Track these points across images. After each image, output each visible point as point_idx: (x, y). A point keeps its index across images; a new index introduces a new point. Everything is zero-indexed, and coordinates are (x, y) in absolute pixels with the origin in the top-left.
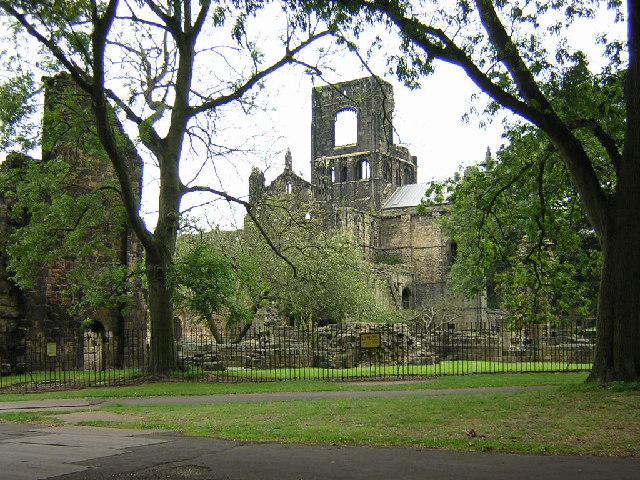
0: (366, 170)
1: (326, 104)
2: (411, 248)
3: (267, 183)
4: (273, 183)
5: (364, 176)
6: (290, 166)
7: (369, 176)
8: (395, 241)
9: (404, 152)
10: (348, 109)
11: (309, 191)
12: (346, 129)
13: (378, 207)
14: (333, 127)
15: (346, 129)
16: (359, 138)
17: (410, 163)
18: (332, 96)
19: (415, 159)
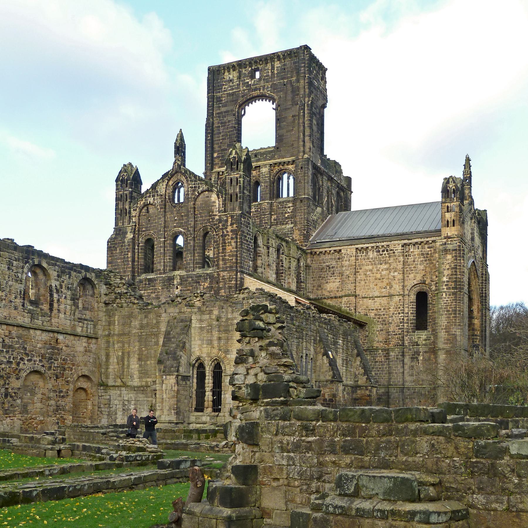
0: (288, 186)
3: (145, 187)
4: (154, 186)
5: (285, 195)
6: (183, 160)
7: (291, 194)
8: (332, 285)
9: (336, 166)
10: (262, 97)
11: (214, 197)
12: (259, 125)
13: (306, 237)
14: (239, 123)
15: (259, 125)
16: (279, 138)
17: (344, 184)
18: (239, 78)
19: (349, 180)
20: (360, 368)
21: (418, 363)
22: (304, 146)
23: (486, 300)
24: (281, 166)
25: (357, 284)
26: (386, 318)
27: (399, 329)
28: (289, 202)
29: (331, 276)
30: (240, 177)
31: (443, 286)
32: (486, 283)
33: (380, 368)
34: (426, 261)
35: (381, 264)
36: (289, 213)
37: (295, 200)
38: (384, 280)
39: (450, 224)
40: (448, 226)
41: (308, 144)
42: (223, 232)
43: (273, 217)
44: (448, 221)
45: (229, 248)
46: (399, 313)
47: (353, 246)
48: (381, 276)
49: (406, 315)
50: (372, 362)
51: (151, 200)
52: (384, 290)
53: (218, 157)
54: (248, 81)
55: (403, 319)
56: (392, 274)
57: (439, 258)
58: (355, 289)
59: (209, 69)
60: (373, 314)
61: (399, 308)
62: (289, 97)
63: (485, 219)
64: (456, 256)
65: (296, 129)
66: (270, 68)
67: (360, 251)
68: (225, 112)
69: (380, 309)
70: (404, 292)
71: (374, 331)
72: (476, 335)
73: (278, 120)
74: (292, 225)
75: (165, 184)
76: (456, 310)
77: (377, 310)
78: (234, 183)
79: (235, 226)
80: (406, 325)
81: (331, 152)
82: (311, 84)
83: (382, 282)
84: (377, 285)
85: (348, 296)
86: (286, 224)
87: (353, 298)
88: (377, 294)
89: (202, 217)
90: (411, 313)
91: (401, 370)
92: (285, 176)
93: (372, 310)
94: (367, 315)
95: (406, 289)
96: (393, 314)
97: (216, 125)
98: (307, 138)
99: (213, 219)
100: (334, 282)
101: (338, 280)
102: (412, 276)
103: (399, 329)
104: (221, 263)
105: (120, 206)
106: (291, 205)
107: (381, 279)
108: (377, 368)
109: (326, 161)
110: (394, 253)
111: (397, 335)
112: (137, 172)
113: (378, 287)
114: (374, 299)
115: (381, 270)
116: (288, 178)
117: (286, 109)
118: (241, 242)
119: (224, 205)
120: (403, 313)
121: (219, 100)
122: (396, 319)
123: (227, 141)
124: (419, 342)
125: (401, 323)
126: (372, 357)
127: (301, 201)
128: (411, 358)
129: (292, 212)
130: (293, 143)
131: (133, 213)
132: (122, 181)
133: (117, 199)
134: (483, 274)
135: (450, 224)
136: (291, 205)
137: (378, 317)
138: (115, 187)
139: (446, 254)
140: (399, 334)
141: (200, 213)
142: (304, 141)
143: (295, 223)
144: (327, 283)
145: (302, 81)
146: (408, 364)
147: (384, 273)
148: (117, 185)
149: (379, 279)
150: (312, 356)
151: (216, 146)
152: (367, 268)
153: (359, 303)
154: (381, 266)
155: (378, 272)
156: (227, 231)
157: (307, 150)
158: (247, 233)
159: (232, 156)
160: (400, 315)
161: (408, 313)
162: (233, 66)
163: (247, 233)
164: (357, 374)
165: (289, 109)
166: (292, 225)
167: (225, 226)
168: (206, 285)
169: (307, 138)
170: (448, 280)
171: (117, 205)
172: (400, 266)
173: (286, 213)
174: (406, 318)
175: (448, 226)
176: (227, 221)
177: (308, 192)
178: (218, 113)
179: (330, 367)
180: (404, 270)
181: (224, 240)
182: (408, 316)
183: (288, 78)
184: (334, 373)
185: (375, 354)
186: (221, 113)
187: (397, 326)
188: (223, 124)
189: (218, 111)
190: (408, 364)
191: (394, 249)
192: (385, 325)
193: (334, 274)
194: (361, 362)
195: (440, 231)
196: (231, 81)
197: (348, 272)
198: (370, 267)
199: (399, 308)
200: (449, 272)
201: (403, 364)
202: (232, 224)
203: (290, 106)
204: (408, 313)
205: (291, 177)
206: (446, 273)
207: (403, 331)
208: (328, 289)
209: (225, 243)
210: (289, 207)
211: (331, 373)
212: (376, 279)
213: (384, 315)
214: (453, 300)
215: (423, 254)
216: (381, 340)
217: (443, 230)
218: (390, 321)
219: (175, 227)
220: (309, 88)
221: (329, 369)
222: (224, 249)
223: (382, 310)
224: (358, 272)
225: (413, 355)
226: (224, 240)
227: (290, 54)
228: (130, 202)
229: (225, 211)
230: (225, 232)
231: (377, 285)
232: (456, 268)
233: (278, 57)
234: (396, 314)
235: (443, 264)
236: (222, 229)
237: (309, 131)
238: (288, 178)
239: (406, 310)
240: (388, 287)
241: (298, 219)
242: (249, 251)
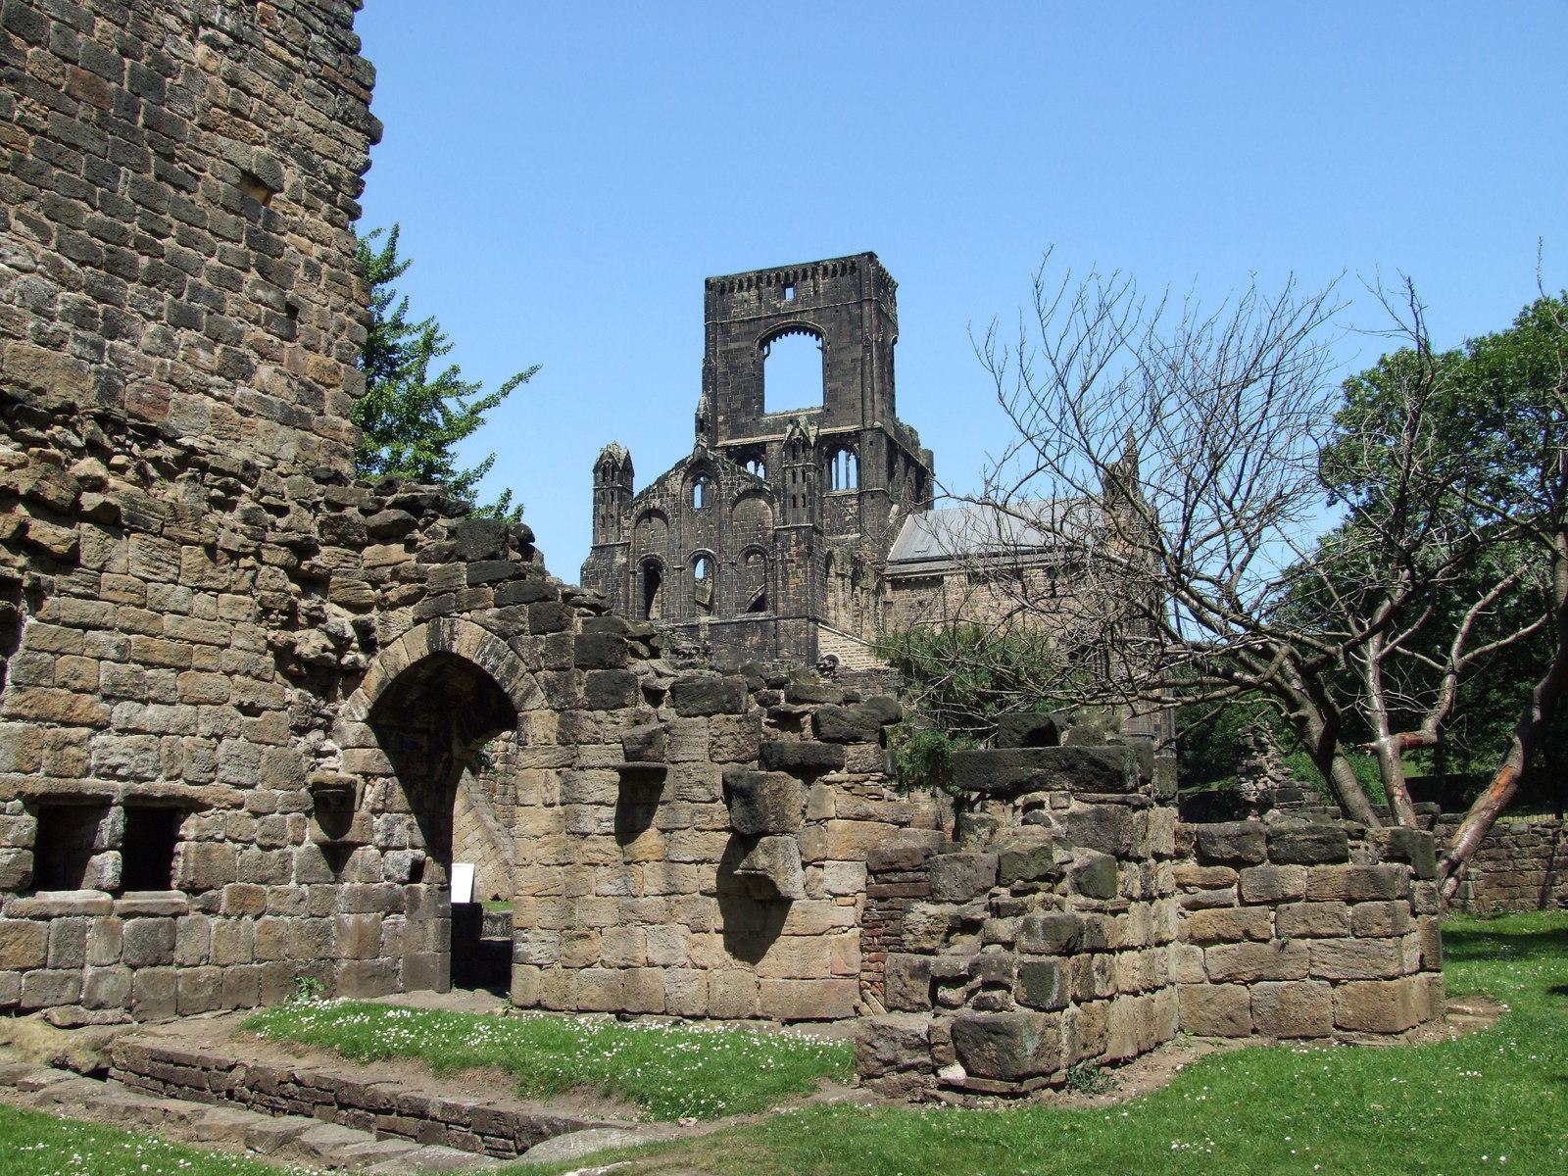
1: (741, 318)
3: (639, 485)
4: (662, 481)
7: (853, 484)
10: (800, 328)
12: (794, 378)
15: (794, 378)
16: (830, 395)
17: (922, 462)
18: (760, 299)
19: (930, 455)
22: (873, 409)
28: (850, 496)
37: (860, 496)
45: (793, 582)
51: (656, 503)
53: (725, 422)
59: (707, 282)
62: (846, 329)
68: (737, 350)
74: (858, 535)
75: (680, 477)
78: (799, 479)
81: (905, 414)
82: (879, 311)
89: (744, 531)
92: (842, 454)
97: (721, 370)
98: (877, 397)
99: (764, 534)
104: (781, 604)
105: (602, 511)
109: (898, 427)
112: (628, 459)
116: (848, 459)
118: (813, 572)
119: (783, 512)
121: (726, 331)
123: (741, 396)
131: (625, 523)
132: (604, 471)
133: (595, 501)
136: (854, 502)
138: (592, 482)
141: (742, 526)
148: (596, 478)
151: (721, 404)
157: (877, 413)
162: (749, 280)
166: (858, 535)
167: (786, 548)
168: (756, 639)
169: (877, 397)
171: (596, 510)
176: (788, 538)
177: (878, 479)
181: (785, 569)
183: (841, 300)
186: (730, 351)
188: (734, 369)
202: (798, 544)
205: (852, 457)
209: (787, 573)
219: (698, 546)
220: (878, 318)
222: (785, 583)
226: (785, 569)
228: (619, 506)
229: (785, 523)
233: (825, 268)
236: (782, 551)
238: (848, 459)
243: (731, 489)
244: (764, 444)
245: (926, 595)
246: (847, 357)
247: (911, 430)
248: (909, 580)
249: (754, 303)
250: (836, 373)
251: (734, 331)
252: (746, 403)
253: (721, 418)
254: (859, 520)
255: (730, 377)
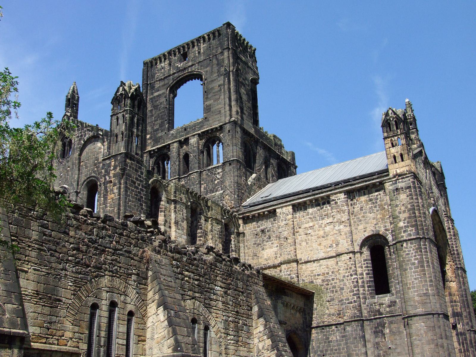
2: (297, 261)
20: (265, 337)
21: (385, 338)
23: (459, 258)
24: (210, 135)
25: (298, 246)
26: (336, 283)
27: (354, 295)
29: (267, 241)
30: (127, 114)
31: (400, 233)
32: (455, 239)
33: (336, 350)
34: (375, 207)
35: (323, 219)
36: (218, 179)
38: (329, 237)
39: (399, 159)
40: (396, 162)
41: (234, 109)
42: (105, 179)
43: (203, 186)
44: (395, 157)
46: (351, 275)
47: (288, 204)
48: (325, 233)
49: (361, 277)
50: (325, 342)
52: (329, 249)
53: (151, 138)
54: (177, 65)
55: (357, 282)
56: (337, 228)
57: (391, 200)
58: (295, 252)
60: (320, 281)
61: (351, 268)
62: (215, 69)
63: (440, 171)
64: (411, 195)
65: (222, 97)
66: (197, 50)
67: (297, 208)
68: (157, 96)
69: (328, 273)
70: (353, 247)
71: (323, 301)
72: (455, 301)
73: (206, 92)
76: (423, 262)
77: (324, 274)
79: (118, 168)
80: (361, 289)
83: (327, 239)
84: (320, 244)
85: (288, 262)
86: (216, 191)
87: (295, 264)
88: (322, 255)
90: (367, 274)
91: (363, 350)
93: (318, 275)
94: (312, 282)
95: (355, 244)
96: (344, 276)
100: (271, 248)
101: (276, 245)
102: (361, 227)
103: (354, 295)
106: (220, 170)
107: (325, 236)
108: (332, 350)
110: (336, 203)
111: (351, 303)
113: (322, 247)
114: (319, 262)
115: (323, 226)
117: (212, 81)
120: (356, 274)
122: (349, 284)
123: (159, 122)
124: (382, 310)
125: (355, 287)
126: (324, 335)
127: (230, 164)
128: (375, 332)
129: (221, 178)
130: (221, 109)
134: (449, 228)
135: (399, 159)
137: (326, 283)
139: (399, 194)
140: (355, 302)
142: (230, 106)
143: (224, 189)
144: (263, 249)
145: (226, 53)
146: (372, 340)
147: (328, 229)
149: (323, 237)
150: (130, 307)
152: (307, 225)
153: (301, 268)
154: (324, 221)
155: (321, 229)
156: (110, 177)
158: (137, 179)
159: (119, 93)
160: (353, 277)
161: (362, 274)
162: (164, 55)
163: (137, 179)
164: (261, 348)
165: (215, 80)
166: (222, 192)
169: (233, 103)
170: (406, 224)
172: (345, 217)
173: (215, 180)
174: (360, 281)
175: (396, 162)
178: (151, 99)
179: (170, 329)
180: (350, 222)
182: (362, 278)
184: (176, 340)
185: (327, 332)
187: (350, 292)
189: (152, 96)
190: (372, 340)
191: (336, 199)
192: (336, 292)
193: (270, 238)
194: (265, 325)
195: (387, 171)
196: (163, 68)
197: (285, 234)
198: (311, 224)
199: (351, 268)
200: (406, 215)
201: (365, 341)
203: (216, 78)
204: (362, 274)
206: (402, 216)
207: (359, 297)
208: (265, 257)
209: (107, 192)
210: (218, 173)
211: (171, 341)
212: (319, 237)
213: (333, 279)
214: (417, 249)
215: (371, 200)
216: (332, 311)
217: (390, 167)
218: (342, 286)
221: (168, 332)
223: (330, 273)
224: (297, 232)
225: (376, 328)
227: (216, 34)
230: (108, 178)
231: (320, 244)
232: (414, 209)
234: (348, 276)
235: (397, 206)
237: (235, 96)
239: (359, 271)
240: (334, 245)
241: (227, 183)
242: (139, 200)
243: (80, 140)
244: (169, 145)
245: (266, 224)
246: (215, 85)
247: (275, 136)
248: (254, 216)
249: (167, 68)
250: (209, 96)
251: (157, 85)
252: (162, 125)
253: (148, 136)
254: (222, 182)
255: (154, 112)
